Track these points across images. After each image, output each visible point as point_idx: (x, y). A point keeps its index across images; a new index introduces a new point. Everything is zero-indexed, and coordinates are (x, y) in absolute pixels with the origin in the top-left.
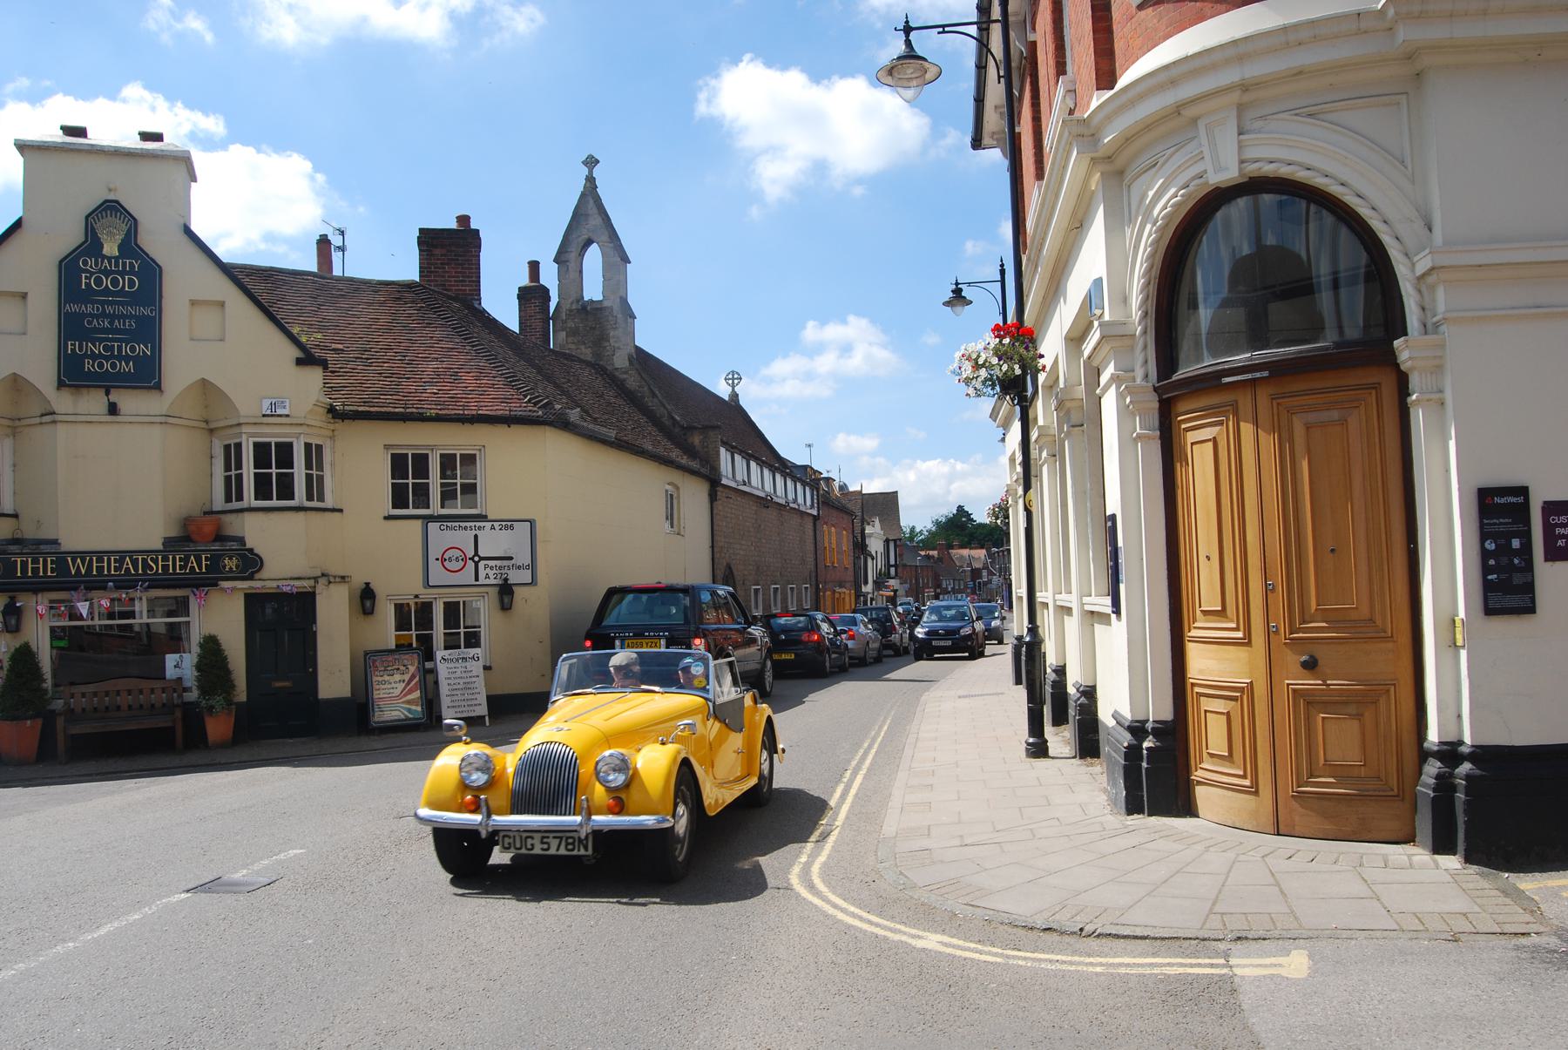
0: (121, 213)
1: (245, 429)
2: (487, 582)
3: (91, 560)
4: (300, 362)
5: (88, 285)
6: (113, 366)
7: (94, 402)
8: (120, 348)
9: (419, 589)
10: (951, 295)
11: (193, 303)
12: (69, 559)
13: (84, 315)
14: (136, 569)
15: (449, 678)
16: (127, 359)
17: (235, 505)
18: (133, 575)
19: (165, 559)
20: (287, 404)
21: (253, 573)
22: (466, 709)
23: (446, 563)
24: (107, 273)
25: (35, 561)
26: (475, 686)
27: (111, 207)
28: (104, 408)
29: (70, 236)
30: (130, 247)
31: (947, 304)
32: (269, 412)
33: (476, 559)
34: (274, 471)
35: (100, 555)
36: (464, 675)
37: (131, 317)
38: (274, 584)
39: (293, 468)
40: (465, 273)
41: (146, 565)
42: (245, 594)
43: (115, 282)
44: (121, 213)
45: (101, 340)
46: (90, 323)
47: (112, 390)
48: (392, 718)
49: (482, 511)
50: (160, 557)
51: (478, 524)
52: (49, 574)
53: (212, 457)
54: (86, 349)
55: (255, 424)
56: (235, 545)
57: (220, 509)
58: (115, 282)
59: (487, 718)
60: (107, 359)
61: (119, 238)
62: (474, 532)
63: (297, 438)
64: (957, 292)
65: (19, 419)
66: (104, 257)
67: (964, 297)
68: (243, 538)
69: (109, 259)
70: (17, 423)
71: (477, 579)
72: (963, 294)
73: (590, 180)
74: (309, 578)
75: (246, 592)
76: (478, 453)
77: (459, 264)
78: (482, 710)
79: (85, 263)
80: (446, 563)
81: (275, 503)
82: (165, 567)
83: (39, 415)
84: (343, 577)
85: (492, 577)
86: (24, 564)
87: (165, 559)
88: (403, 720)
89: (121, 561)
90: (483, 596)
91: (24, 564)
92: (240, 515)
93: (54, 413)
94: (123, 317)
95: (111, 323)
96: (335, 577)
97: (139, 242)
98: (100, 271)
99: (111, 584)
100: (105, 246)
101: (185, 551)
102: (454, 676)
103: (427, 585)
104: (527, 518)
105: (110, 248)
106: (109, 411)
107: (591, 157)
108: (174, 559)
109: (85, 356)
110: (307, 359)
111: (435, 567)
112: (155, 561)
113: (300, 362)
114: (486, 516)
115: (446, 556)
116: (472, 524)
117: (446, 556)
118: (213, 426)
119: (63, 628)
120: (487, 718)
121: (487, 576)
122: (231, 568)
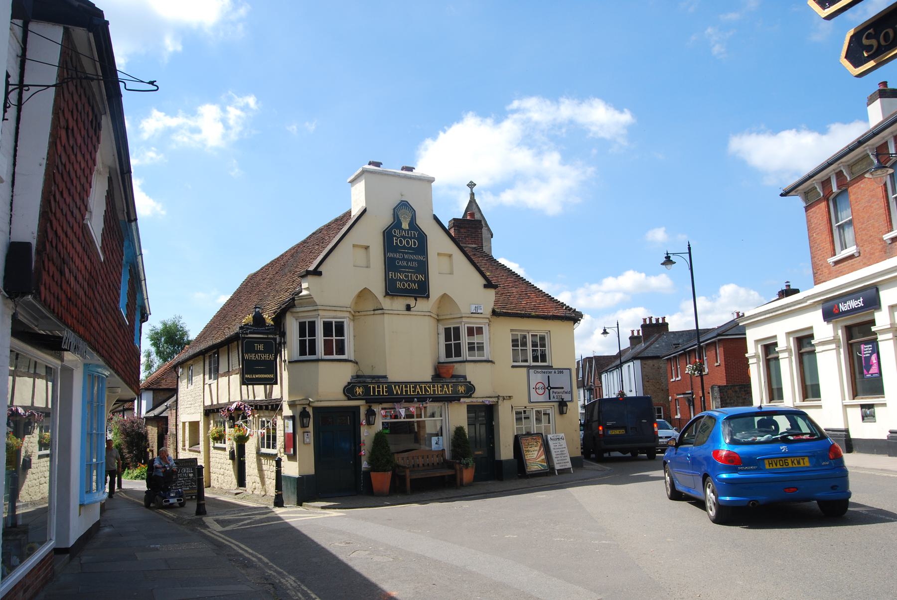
0: (409, 208)
1: (464, 320)
2: (554, 400)
3: (402, 386)
4: (485, 286)
5: (396, 243)
6: (409, 285)
7: (399, 303)
8: (411, 276)
9: (526, 403)
10: (665, 259)
11: (439, 254)
12: (393, 386)
13: (396, 259)
14: (422, 392)
15: (555, 449)
16: (414, 282)
17: (454, 359)
18: (448, 394)
19: (434, 387)
20: (482, 307)
21: (471, 394)
22: (564, 464)
23: (537, 390)
24: (404, 237)
25: (379, 387)
26: (564, 453)
27: (404, 205)
28: (404, 308)
29: (386, 220)
30: (413, 225)
31: (662, 264)
32: (474, 312)
33: (549, 388)
34: (334, 338)
35: (406, 384)
36: (560, 447)
37: (415, 260)
38: (481, 400)
39: (315, 336)
40: (476, 242)
41: (426, 390)
42: (467, 405)
43: (408, 243)
44: (409, 208)
45: (404, 272)
46: (398, 263)
47: (418, 299)
48: (535, 469)
49: (549, 364)
50: (404, 386)
51: (549, 370)
52: (385, 394)
53: (438, 334)
54: (397, 277)
55: (468, 317)
56: (462, 380)
57: (443, 361)
58: (408, 243)
59: (572, 469)
60: (406, 281)
61: (409, 220)
62: (548, 375)
63: (485, 325)
64: (668, 258)
65: (359, 312)
66: (403, 229)
67: (672, 260)
68: (465, 376)
69: (405, 230)
70: (357, 314)
71: (550, 399)
72: (671, 259)
73: (472, 194)
74: (494, 397)
75: (468, 404)
76: (546, 334)
77: (472, 237)
78: (569, 465)
79: (395, 232)
80: (537, 390)
81: (335, 357)
82: (434, 391)
83: (372, 309)
84: (510, 397)
85: (556, 397)
86: (374, 388)
87: (434, 387)
88: (539, 470)
89: (415, 387)
90: (551, 408)
91: (374, 388)
92: (463, 364)
93: (383, 309)
94: (412, 260)
95: (407, 263)
96: (507, 397)
97: (417, 223)
98: (401, 237)
99: (415, 399)
100: (403, 224)
101: (442, 382)
102: (556, 448)
103: (530, 402)
104: (568, 367)
105: (405, 226)
106: (407, 308)
107: (471, 182)
108: (437, 386)
109: (397, 280)
110: (489, 285)
111: (533, 391)
112: (429, 387)
113: (485, 286)
114: (552, 367)
115: (537, 387)
116: (547, 370)
117: (537, 387)
118: (441, 318)
119: (387, 423)
120: (572, 469)
121: (554, 398)
122: (462, 392)
